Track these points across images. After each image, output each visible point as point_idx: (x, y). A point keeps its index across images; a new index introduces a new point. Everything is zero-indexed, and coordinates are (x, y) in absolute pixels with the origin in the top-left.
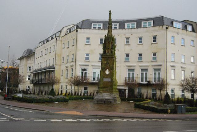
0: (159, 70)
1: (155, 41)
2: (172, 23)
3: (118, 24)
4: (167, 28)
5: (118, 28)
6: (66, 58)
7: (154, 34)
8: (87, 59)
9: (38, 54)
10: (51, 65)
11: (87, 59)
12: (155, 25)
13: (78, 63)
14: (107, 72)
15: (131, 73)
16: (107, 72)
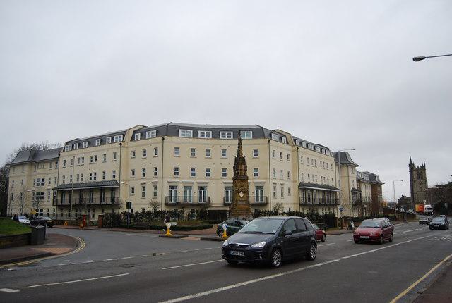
0: (262, 187)
1: (256, 155)
2: (270, 135)
3: (211, 132)
4: (269, 142)
5: (211, 137)
6: (139, 173)
7: (255, 147)
8: (177, 174)
9: (68, 163)
10: (109, 178)
11: (177, 174)
12: (254, 137)
13: (164, 180)
14: (241, 195)
15: (188, 190)
16: (241, 195)
